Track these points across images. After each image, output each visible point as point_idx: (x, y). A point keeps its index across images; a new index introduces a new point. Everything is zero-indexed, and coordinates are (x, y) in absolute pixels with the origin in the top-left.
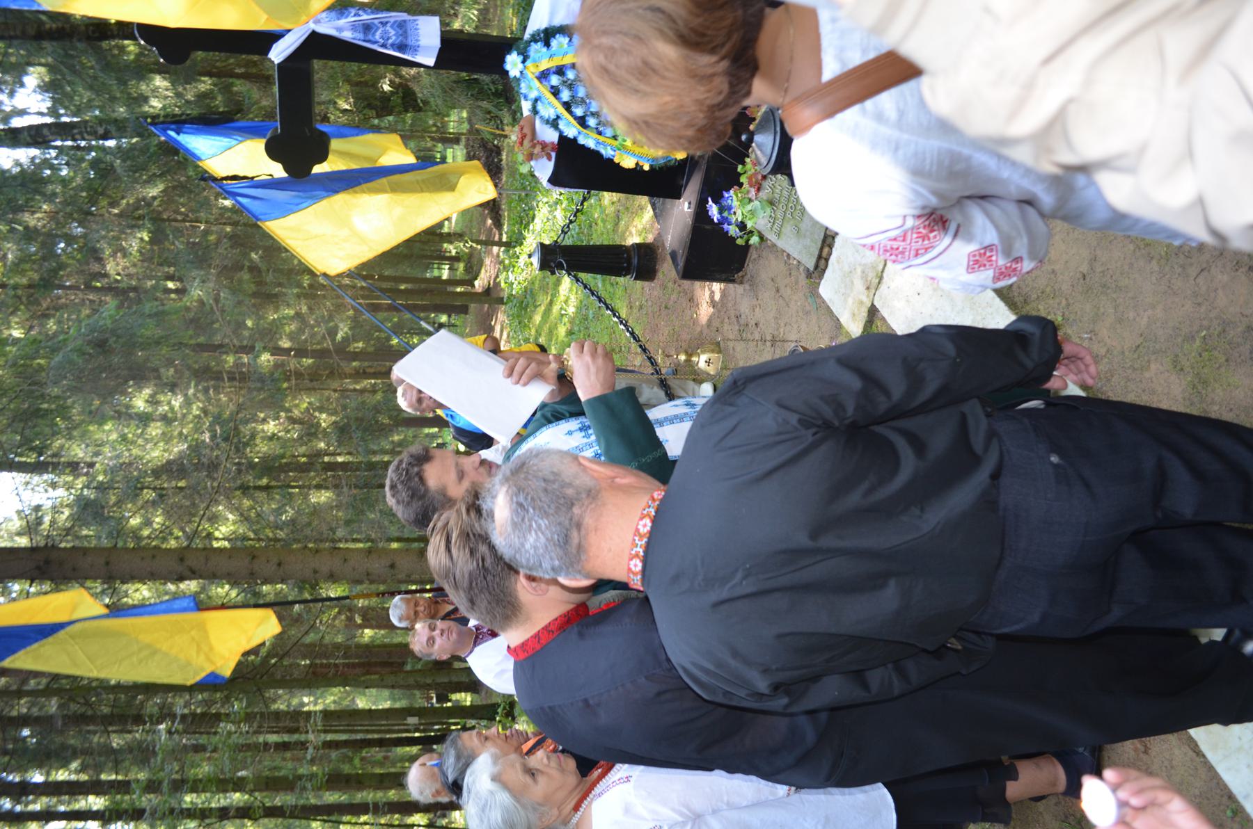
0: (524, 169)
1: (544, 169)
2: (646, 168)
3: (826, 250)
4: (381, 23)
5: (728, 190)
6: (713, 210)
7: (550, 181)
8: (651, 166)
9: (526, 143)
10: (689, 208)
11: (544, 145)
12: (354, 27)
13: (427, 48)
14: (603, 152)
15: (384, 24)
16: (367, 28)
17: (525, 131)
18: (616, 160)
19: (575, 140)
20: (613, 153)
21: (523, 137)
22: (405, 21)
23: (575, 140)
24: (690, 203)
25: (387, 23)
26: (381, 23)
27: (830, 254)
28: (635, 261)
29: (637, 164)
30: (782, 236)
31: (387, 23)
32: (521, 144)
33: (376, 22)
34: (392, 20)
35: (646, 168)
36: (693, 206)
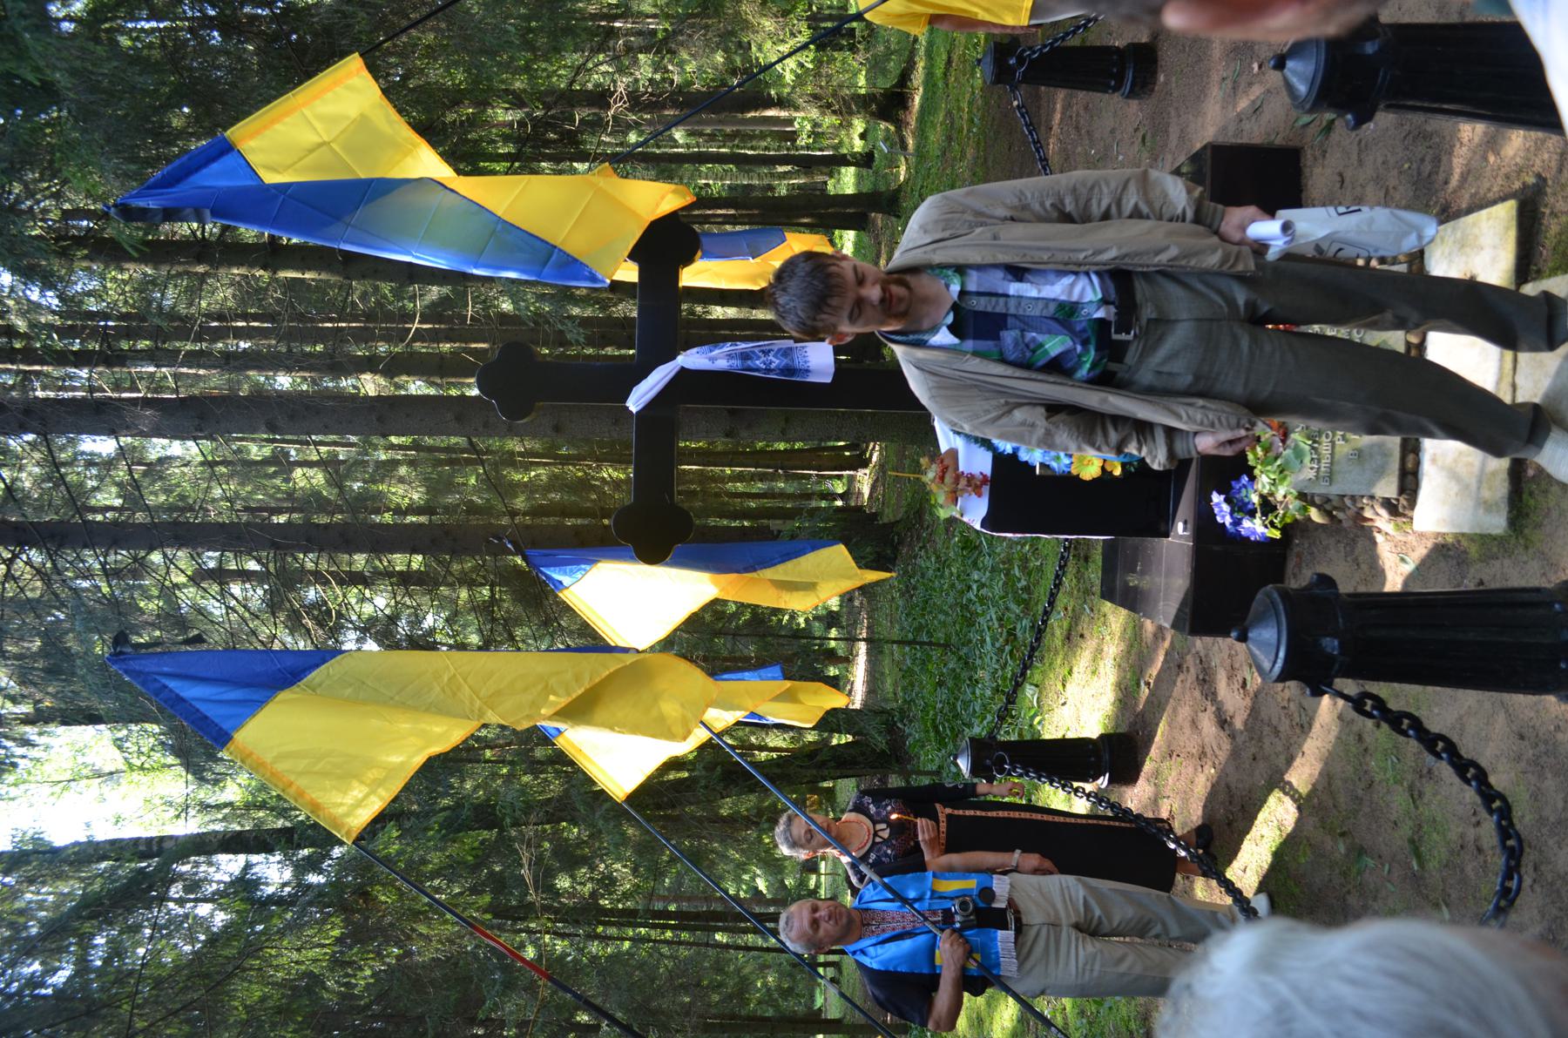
0: (943, 514)
1: (975, 511)
2: (1118, 472)
3: (1411, 457)
4: (763, 352)
5: (1238, 479)
6: (1222, 511)
7: (982, 526)
8: (1123, 465)
9: (948, 479)
10: (1185, 530)
11: (970, 478)
12: (730, 356)
13: (820, 373)
14: (1054, 465)
15: (766, 353)
16: (745, 356)
17: (946, 463)
18: (1074, 472)
19: (1014, 455)
20: (1067, 461)
21: (944, 471)
22: (791, 349)
23: (1014, 455)
24: (1185, 523)
25: (769, 351)
26: (763, 352)
27: (1418, 463)
28: (1107, 757)
29: (1103, 469)
30: (1337, 477)
31: (769, 351)
32: (942, 478)
33: (756, 350)
34: (775, 348)
35: (1118, 472)
36: (1189, 526)
